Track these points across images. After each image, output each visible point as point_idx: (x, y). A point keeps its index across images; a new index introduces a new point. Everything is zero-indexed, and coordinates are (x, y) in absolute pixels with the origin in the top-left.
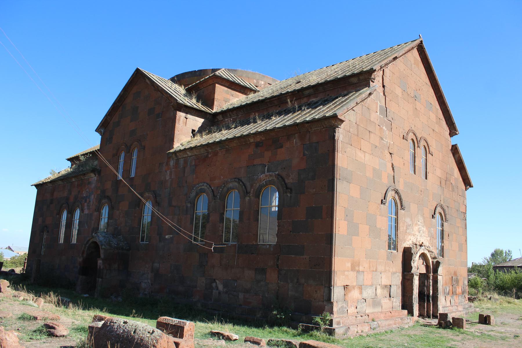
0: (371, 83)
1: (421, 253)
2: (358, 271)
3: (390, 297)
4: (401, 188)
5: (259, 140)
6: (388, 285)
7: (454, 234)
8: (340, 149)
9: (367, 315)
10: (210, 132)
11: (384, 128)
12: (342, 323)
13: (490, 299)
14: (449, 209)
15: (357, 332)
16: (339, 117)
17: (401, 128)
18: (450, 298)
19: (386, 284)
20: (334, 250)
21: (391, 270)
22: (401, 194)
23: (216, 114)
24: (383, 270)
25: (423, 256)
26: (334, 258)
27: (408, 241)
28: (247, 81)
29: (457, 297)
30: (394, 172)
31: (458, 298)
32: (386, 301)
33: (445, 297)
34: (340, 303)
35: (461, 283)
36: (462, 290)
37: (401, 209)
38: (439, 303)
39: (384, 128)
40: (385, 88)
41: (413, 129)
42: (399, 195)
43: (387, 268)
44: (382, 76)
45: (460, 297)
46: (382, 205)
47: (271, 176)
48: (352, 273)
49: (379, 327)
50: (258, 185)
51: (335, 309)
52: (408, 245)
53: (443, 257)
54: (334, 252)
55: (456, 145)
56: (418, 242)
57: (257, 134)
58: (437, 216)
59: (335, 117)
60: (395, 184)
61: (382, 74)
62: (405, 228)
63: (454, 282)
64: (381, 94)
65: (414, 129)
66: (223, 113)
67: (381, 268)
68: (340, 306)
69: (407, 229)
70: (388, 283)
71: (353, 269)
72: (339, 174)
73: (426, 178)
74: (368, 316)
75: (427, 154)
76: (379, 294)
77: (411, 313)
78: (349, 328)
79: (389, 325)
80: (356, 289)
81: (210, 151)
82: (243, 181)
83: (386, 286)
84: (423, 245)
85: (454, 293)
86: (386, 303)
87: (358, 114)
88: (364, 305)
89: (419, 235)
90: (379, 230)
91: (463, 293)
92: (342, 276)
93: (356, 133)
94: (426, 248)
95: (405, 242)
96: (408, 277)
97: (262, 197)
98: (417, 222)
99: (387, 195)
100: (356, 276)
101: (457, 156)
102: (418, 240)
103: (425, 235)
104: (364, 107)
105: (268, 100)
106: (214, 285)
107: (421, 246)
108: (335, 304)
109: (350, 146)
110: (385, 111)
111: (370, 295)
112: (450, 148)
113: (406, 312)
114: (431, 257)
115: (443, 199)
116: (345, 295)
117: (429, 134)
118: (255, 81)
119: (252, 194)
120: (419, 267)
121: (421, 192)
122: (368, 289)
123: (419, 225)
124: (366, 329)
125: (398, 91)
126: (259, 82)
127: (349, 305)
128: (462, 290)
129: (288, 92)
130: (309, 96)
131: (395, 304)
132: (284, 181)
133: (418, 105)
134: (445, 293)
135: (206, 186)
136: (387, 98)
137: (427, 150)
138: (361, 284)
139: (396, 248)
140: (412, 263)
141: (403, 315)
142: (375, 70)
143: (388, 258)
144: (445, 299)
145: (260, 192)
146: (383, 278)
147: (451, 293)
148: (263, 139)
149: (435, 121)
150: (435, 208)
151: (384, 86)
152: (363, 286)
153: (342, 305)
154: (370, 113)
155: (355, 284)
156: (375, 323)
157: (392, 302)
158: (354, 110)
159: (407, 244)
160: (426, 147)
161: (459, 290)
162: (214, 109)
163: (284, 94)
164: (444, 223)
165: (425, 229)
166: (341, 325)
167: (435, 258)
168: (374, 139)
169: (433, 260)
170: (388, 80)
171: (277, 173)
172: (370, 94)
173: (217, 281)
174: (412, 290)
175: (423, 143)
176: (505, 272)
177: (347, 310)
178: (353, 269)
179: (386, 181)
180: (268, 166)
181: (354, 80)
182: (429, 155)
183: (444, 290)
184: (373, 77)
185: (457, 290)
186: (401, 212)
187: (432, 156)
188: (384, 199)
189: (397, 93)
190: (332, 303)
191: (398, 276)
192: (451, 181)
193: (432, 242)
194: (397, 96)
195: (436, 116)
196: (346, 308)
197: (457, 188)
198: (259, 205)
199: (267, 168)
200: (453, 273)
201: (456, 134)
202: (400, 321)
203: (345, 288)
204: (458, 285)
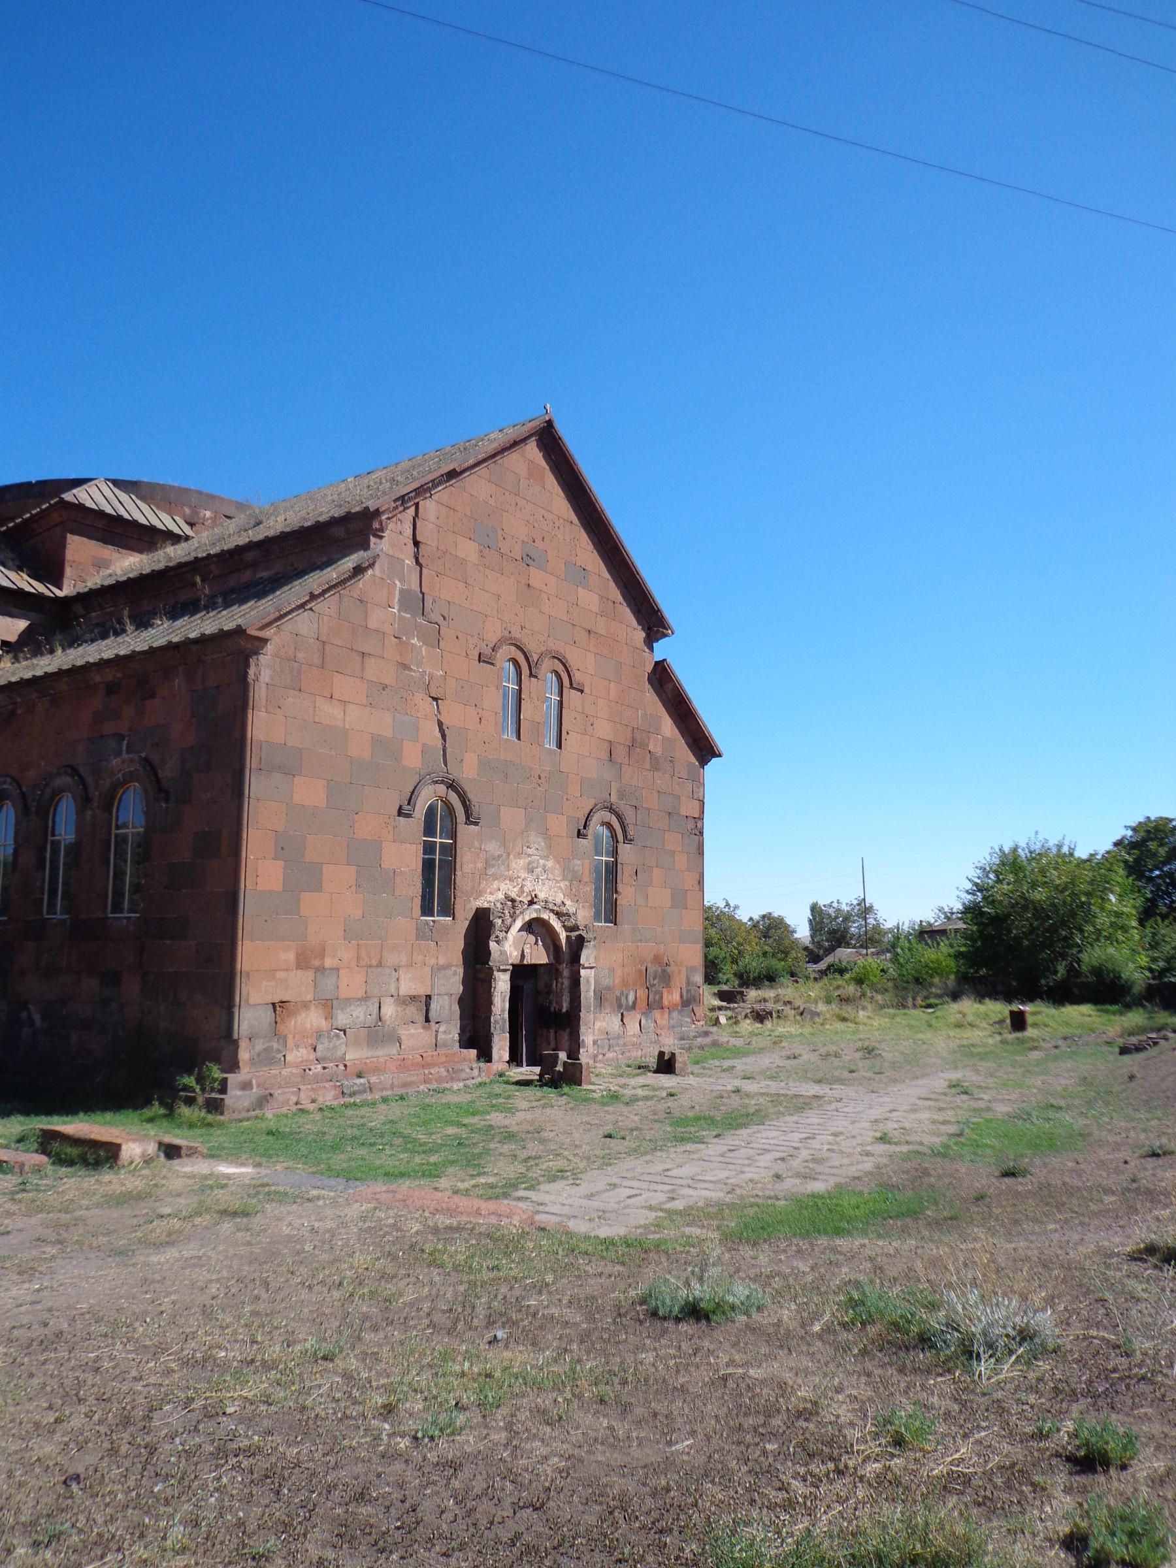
0: (373, 540)
1: (527, 918)
2: (320, 970)
3: (427, 1020)
4: (467, 771)
5: (110, 678)
6: (419, 996)
7: (655, 870)
8: (264, 702)
9: (341, 1067)
10: (37, 652)
11: (415, 641)
12: (258, 1086)
13: (802, 1014)
14: (639, 812)
15: (296, 1104)
16: (248, 632)
17: (472, 636)
18: (639, 1017)
19: (413, 993)
20: (240, 927)
21: (433, 961)
22: (466, 788)
23: (66, 599)
24: (403, 963)
25: (535, 927)
26: (240, 943)
27: (491, 893)
28: (164, 511)
29: (663, 1014)
30: (445, 741)
31: (666, 1016)
32: (412, 1031)
33: (622, 1014)
34: (261, 1041)
35: (679, 981)
36: (681, 996)
37: (466, 823)
38: (583, 1029)
39: (415, 641)
40: (421, 546)
41: (516, 634)
43: (419, 958)
44: (414, 519)
45: (675, 1014)
47: (131, 761)
48: (300, 973)
49: (371, 1089)
50: (108, 782)
51: (244, 1055)
52: (490, 902)
53: (615, 924)
54: (240, 931)
55: (664, 660)
56: (525, 894)
57: (103, 664)
58: (597, 828)
59: (239, 631)
60: (446, 766)
62: (480, 865)
63: (654, 979)
65: (518, 635)
66: (88, 599)
67: (391, 959)
68: (259, 1047)
69: (487, 864)
70: (422, 991)
71: (302, 963)
72: (252, 761)
73: (560, 747)
74: (345, 1066)
75: (564, 689)
76: (391, 1017)
77: (485, 1055)
78: (271, 1095)
79: (405, 1085)
80: (313, 1008)
81: (19, 700)
82: (81, 770)
83: (413, 998)
84: (535, 900)
85: (653, 1005)
86: (415, 1036)
87: (325, 618)
88: (338, 1042)
89: (530, 877)
90: (392, 875)
91: (689, 1002)
92: (264, 983)
93: (317, 660)
94: (551, 906)
95: (480, 896)
96: (482, 976)
97: (117, 812)
98: (525, 848)
99: (415, 793)
100: (314, 981)
101: (669, 686)
102: (526, 889)
103: (550, 876)
104: (345, 599)
105: (172, 573)
106: (24, 1015)
107: (531, 903)
108: (243, 1044)
109: (295, 693)
110: (417, 602)
111: (362, 1018)
113: (473, 1053)
114: (564, 926)
115: (618, 791)
116: (276, 1022)
117: (572, 642)
118: (187, 511)
119: (96, 804)
120: (527, 951)
121: (540, 778)
122: (352, 1007)
123: (530, 855)
124: (328, 1097)
125: (468, 550)
126: (197, 514)
127: (290, 1042)
128: (685, 997)
129: (209, 556)
130: (254, 565)
131: (443, 1036)
132: (156, 774)
133: (537, 576)
134: (620, 1006)
135: (11, 784)
137: (566, 680)
138: (328, 998)
139: (448, 909)
140: (493, 945)
141: (465, 1060)
142: (377, 510)
143: (420, 935)
144: (622, 1020)
145: (113, 798)
146: (402, 982)
147: (642, 1004)
148: (119, 675)
149: (595, 607)
150: (587, 812)
151: (416, 543)
152: (335, 1002)
153: (267, 1045)
154: (367, 612)
155: (309, 997)
156: (362, 1080)
157: (434, 1033)
159: (482, 903)
161: (672, 997)
162: (65, 587)
163: (203, 559)
164: (621, 846)
165: (550, 864)
166: (254, 1090)
167: (575, 928)
168: (381, 670)
169: (568, 934)
170: (431, 526)
171: (143, 755)
172: (358, 570)
173: (30, 1006)
174: (489, 1003)
175: (547, 664)
176: (927, 944)
177: (284, 1056)
178: (302, 963)
179: (412, 759)
180: (128, 741)
181: (339, 532)
183: (618, 999)
184: (378, 527)
185: (665, 997)
186: (464, 831)
187: (582, 691)
188: (409, 804)
189: (461, 554)
190: (235, 1044)
191: (455, 973)
192: (651, 747)
193: (578, 891)
194: (463, 561)
195: (601, 597)
196: (279, 1051)
197: (671, 761)
198: (111, 829)
199: (125, 742)
200: (650, 958)
201: (665, 635)
202: (445, 1074)
203: (278, 1009)
204: (668, 986)
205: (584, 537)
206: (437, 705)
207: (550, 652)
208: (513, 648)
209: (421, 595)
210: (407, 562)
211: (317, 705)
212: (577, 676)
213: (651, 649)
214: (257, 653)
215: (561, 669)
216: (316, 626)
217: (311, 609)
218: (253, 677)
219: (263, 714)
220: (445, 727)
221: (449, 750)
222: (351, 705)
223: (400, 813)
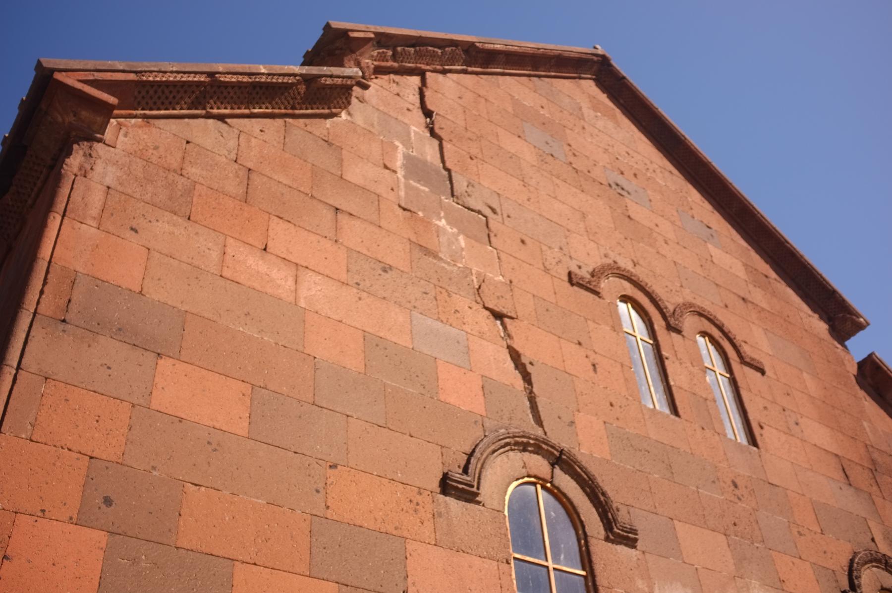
11: (443, 223)
37: (607, 539)
39: (443, 223)
42: (579, 475)
46: (454, 504)
61: (420, 85)
64: (413, 128)
87: (253, 140)
99: (477, 453)
112: (854, 370)
121: (736, 486)
136: (447, 146)
151: (428, 113)
158: (226, 123)
160: (720, 340)
182: (747, 369)
187: (763, 373)
205: (694, 196)
206: (503, 324)
207: (691, 305)
208: (626, 284)
209: (445, 173)
210: (413, 128)
211: (229, 250)
212: (746, 349)
213: (845, 347)
214: (91, 139)
215: (716, 333)
216: (232, 143)
217: (221, 118)
218: (75, 170)
219: (89, 230)
220: (524, 360)
221: (541, 402)
222: (310, 273)
223: (446, 486)
